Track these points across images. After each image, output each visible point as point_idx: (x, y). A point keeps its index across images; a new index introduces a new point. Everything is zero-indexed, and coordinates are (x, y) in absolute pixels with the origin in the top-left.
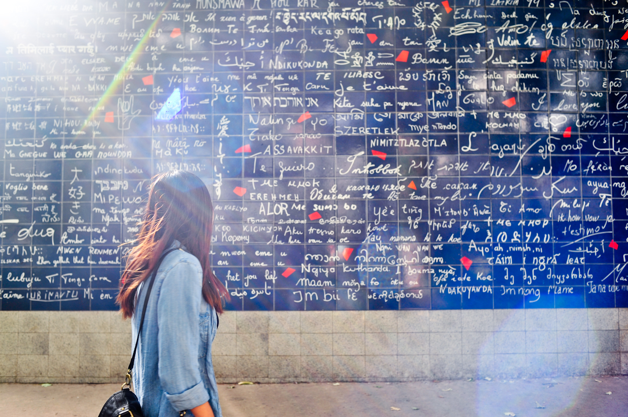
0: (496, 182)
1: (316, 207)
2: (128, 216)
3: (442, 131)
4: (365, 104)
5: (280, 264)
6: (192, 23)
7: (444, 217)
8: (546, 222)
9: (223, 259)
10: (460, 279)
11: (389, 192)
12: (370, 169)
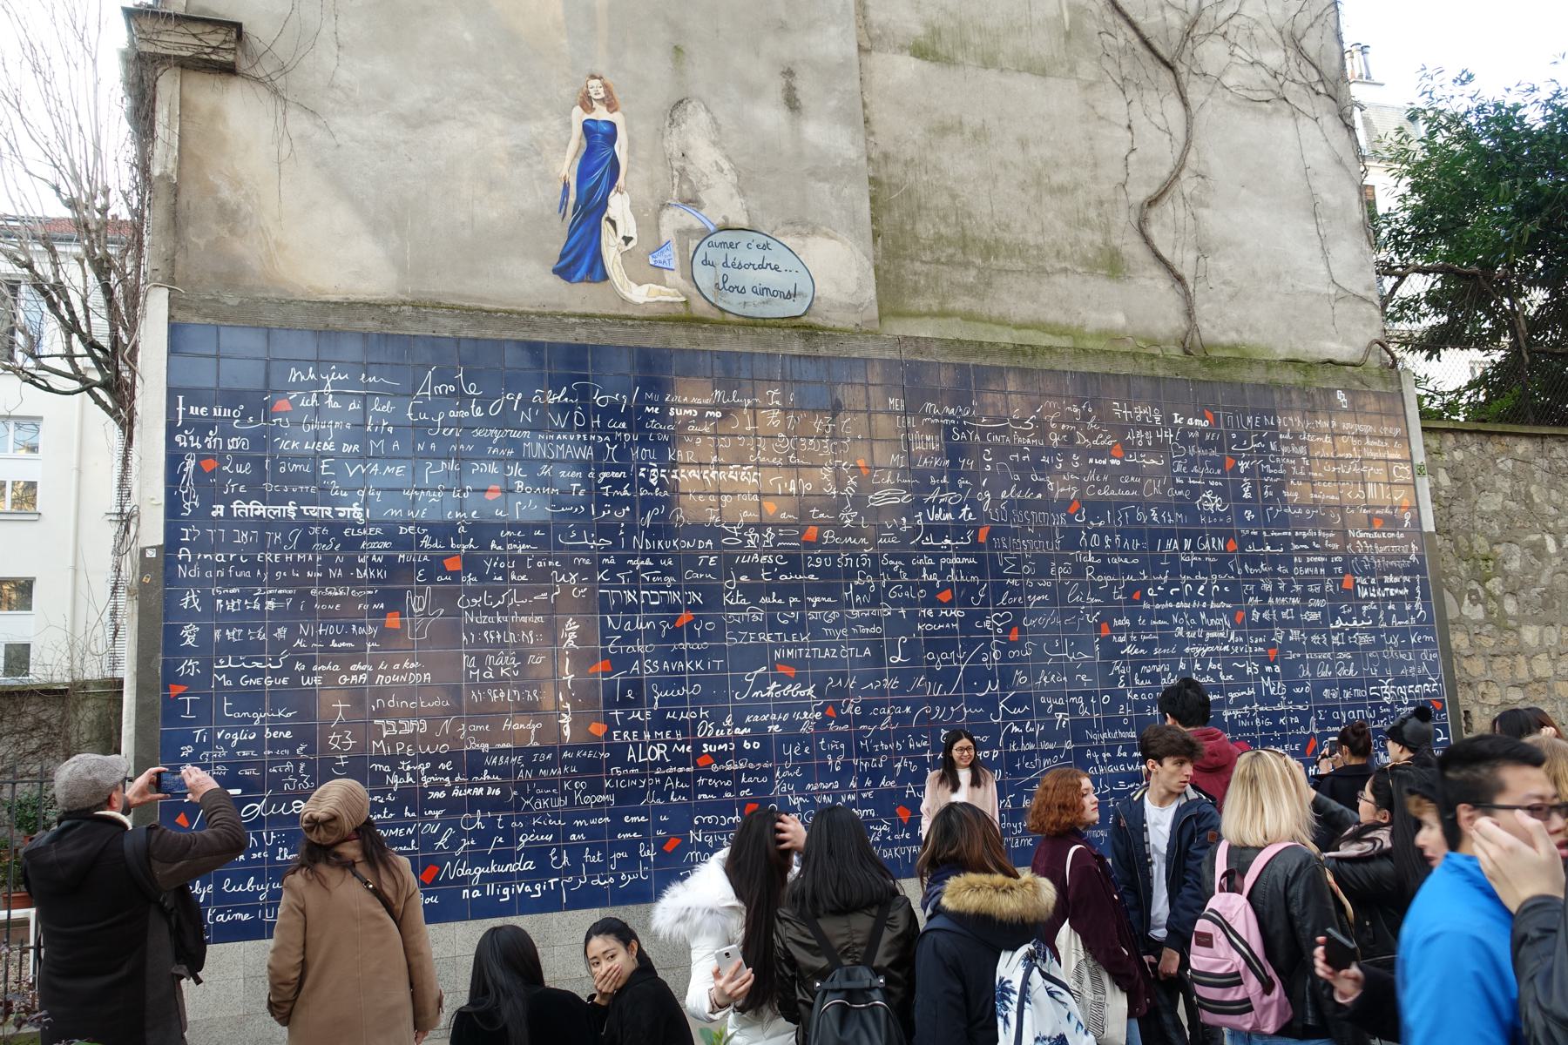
0: (933, 701)
1: (706, 748)
2: (429, 773)
3: (865, 635)
4: (764, 600)
5: (659, 833)
6: (518, 478)
7: (872, 754)
8: (996, 754)
9: (578, 831)
10: (897, 837)
11: (801, 722)
12: (775, 690)
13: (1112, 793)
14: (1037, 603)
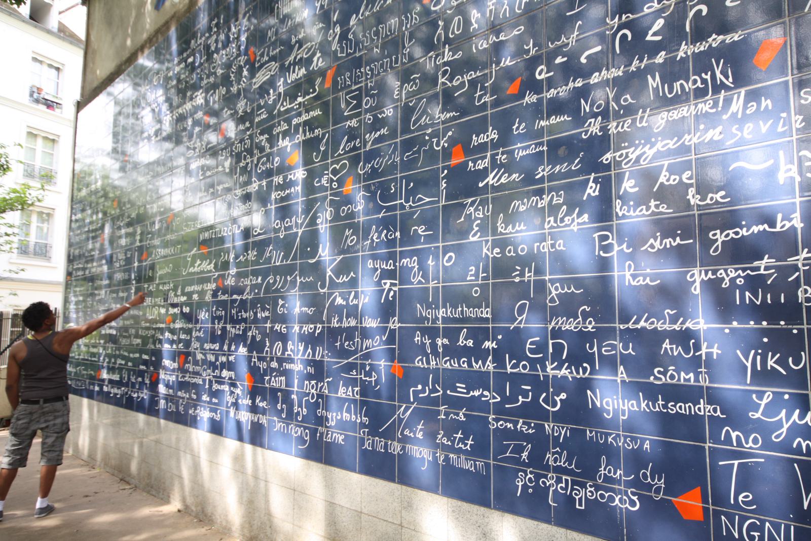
13: (446, 400)
14: (376, 141)
